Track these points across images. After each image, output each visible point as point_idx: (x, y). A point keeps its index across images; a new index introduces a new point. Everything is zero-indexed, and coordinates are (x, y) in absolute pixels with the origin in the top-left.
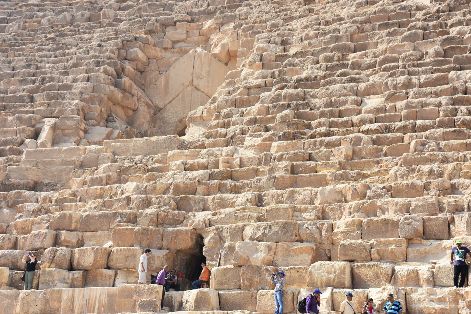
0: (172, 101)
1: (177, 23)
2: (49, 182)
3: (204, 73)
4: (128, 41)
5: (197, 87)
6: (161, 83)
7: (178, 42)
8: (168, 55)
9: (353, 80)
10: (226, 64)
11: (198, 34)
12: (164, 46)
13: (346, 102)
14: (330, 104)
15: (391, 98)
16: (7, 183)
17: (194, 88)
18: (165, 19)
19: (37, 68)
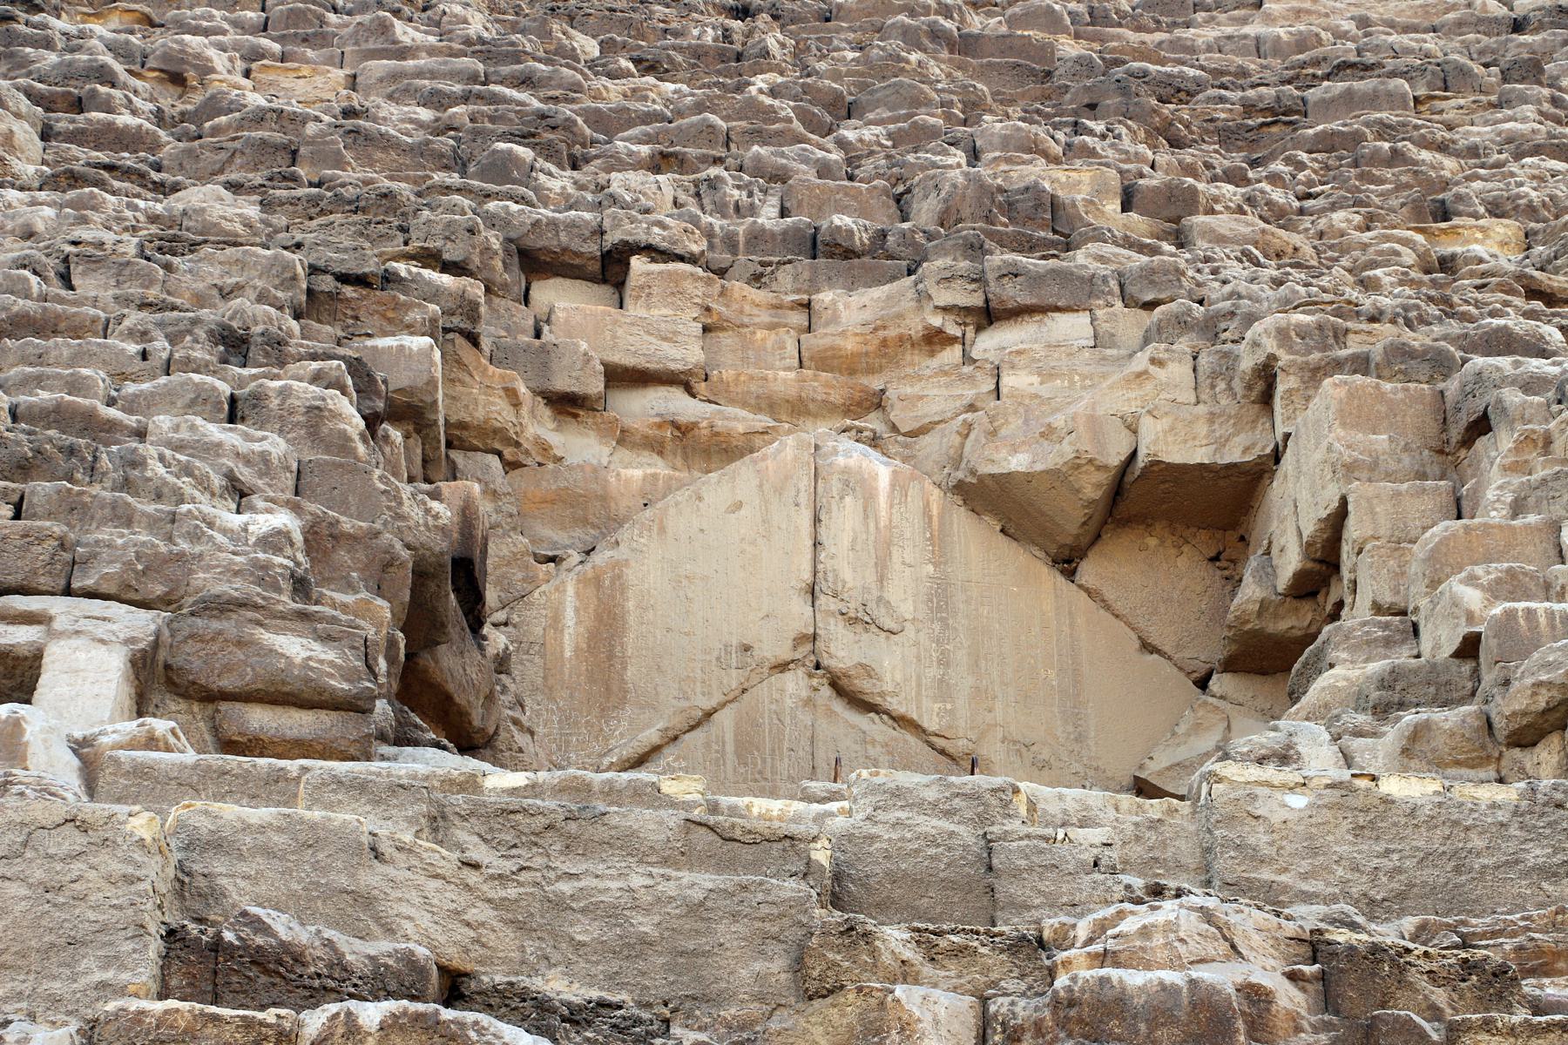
0: (656, 749)
1: (638, 264)
2: (595, 994)
3: (904, 597)
4: (344, 278)
5: (863, 685)
6: (556, 621)
8: (580, 447)
10: (1067, 562)
11: (791, 348)
12: (562, 383)
16: (229, 936)
17: (826, 691)
18: (536, 223)
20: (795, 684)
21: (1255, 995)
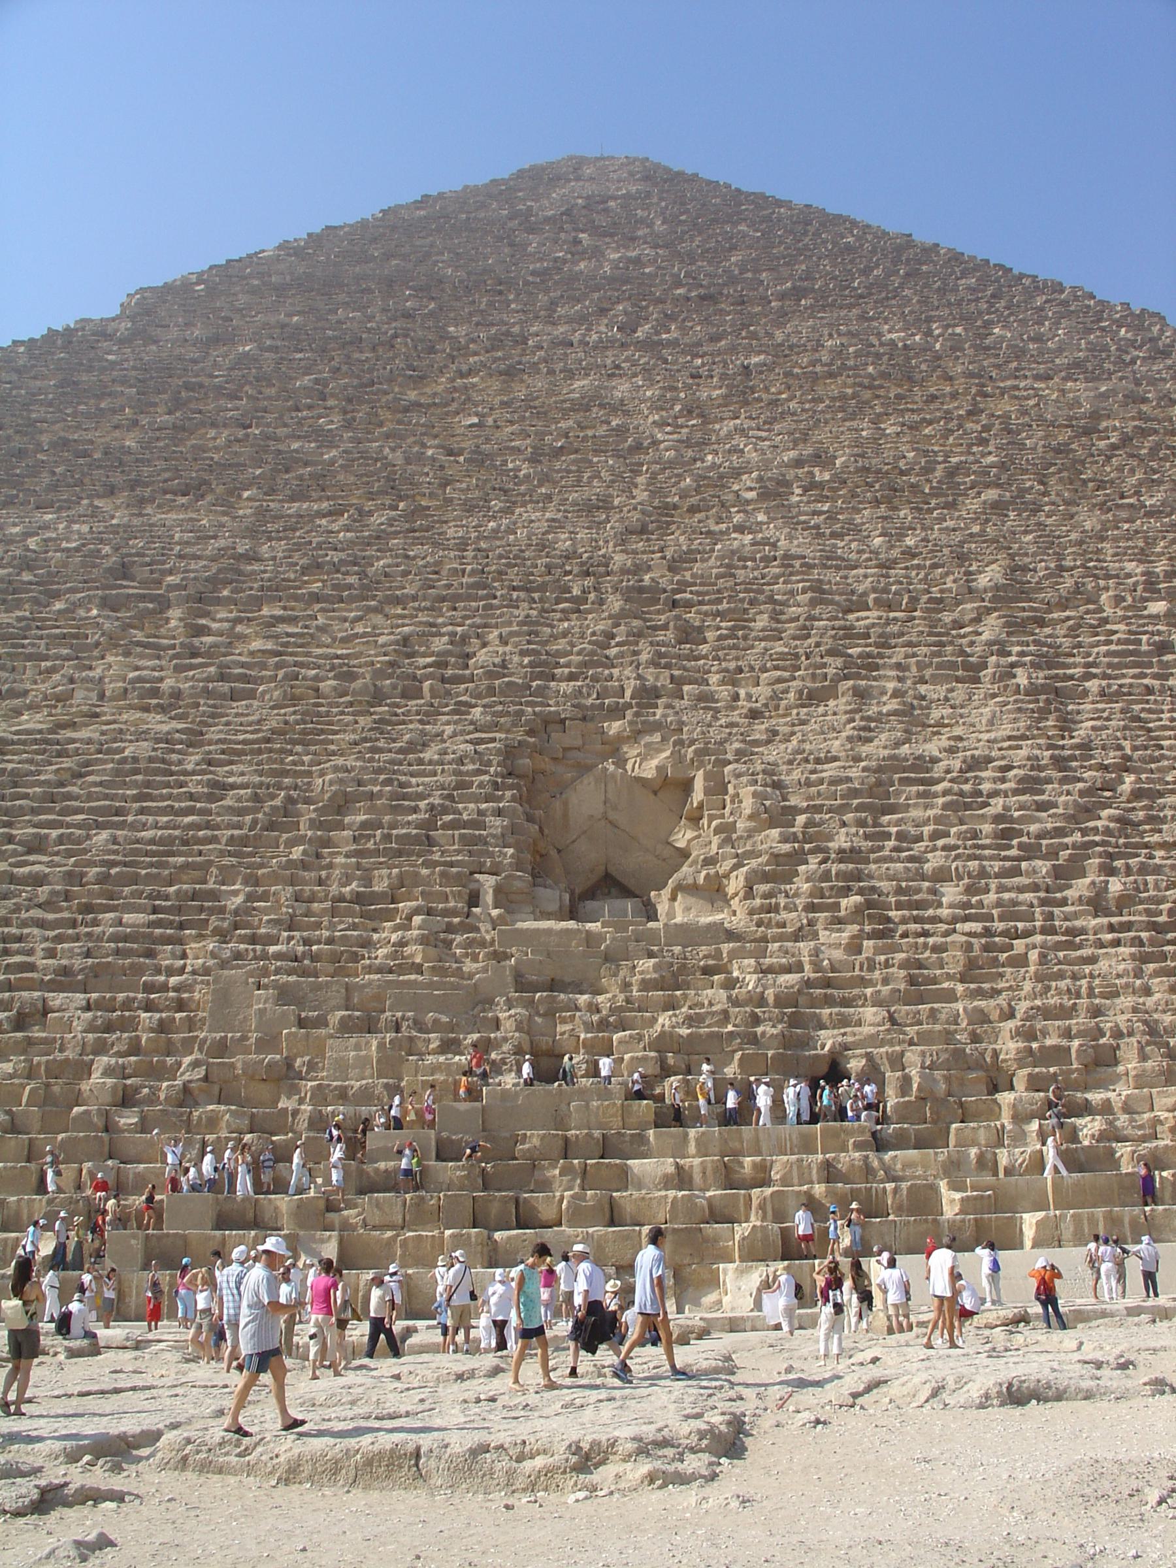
7: (570, 749)
9: (911, 859)
10: (655, 793)
13: (918, 890)
14: (899, 891)
15: (970, 890)
19: (402, 785)
20: (603, 822)
21: (662, 977)
